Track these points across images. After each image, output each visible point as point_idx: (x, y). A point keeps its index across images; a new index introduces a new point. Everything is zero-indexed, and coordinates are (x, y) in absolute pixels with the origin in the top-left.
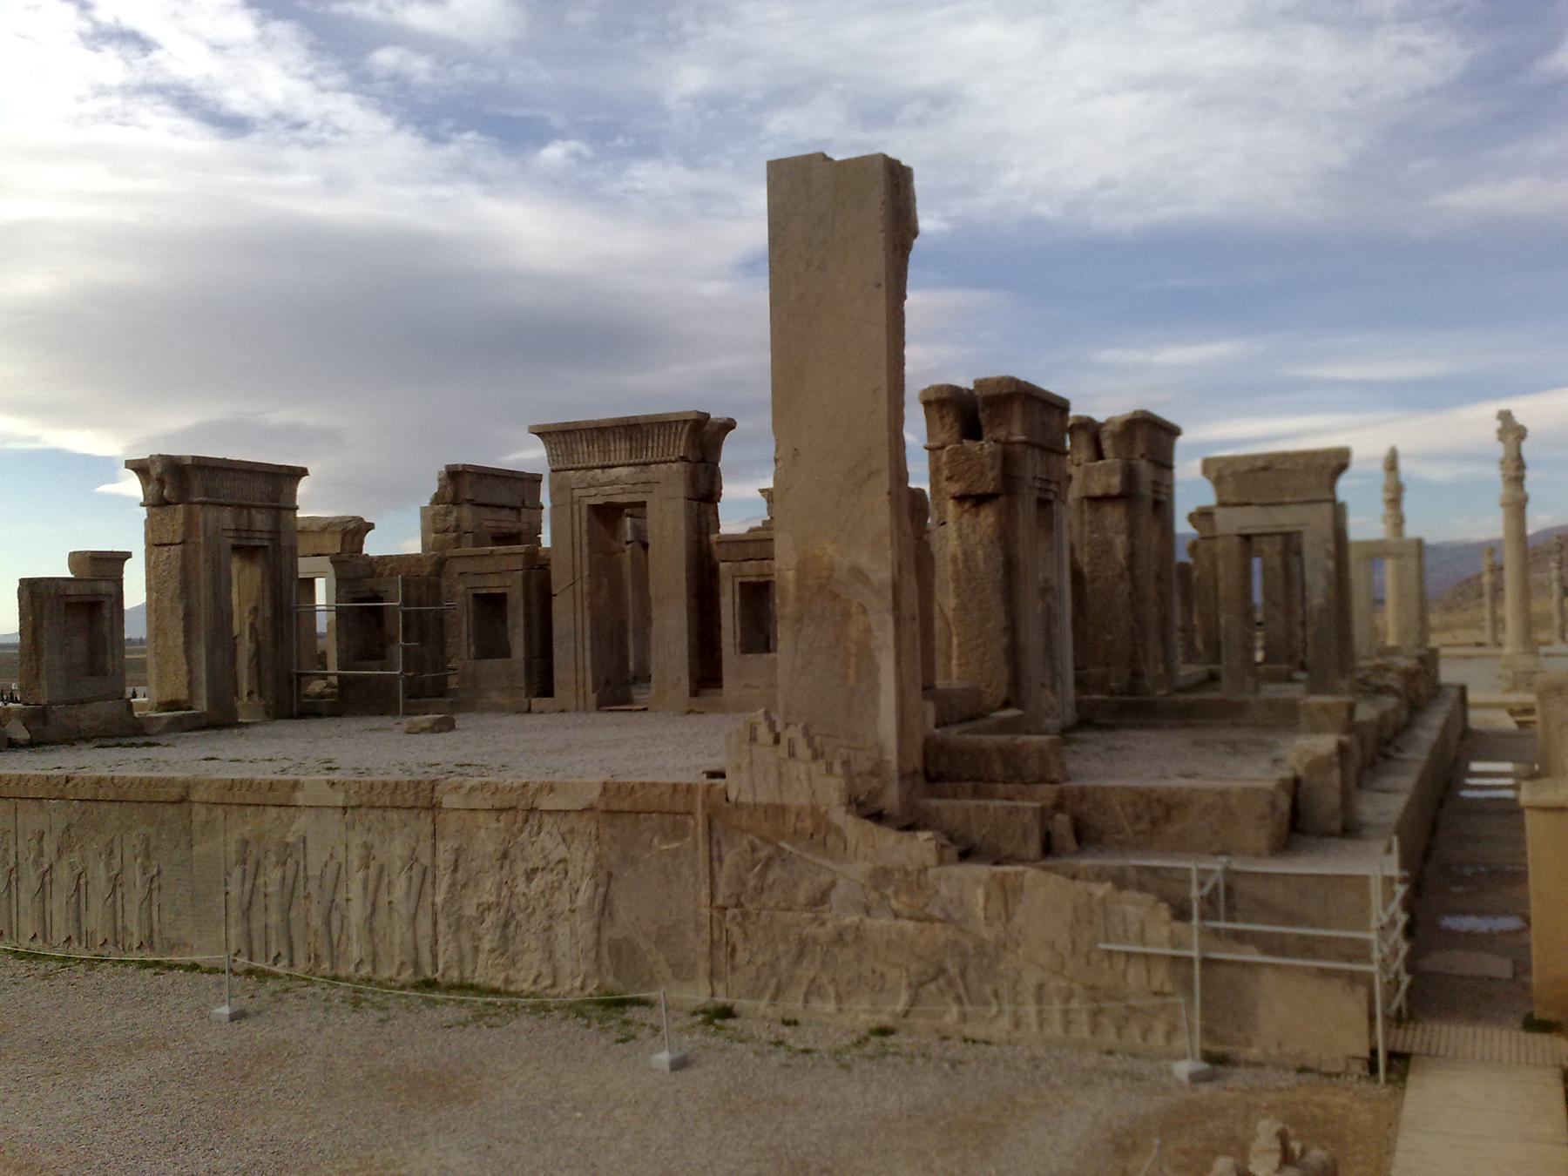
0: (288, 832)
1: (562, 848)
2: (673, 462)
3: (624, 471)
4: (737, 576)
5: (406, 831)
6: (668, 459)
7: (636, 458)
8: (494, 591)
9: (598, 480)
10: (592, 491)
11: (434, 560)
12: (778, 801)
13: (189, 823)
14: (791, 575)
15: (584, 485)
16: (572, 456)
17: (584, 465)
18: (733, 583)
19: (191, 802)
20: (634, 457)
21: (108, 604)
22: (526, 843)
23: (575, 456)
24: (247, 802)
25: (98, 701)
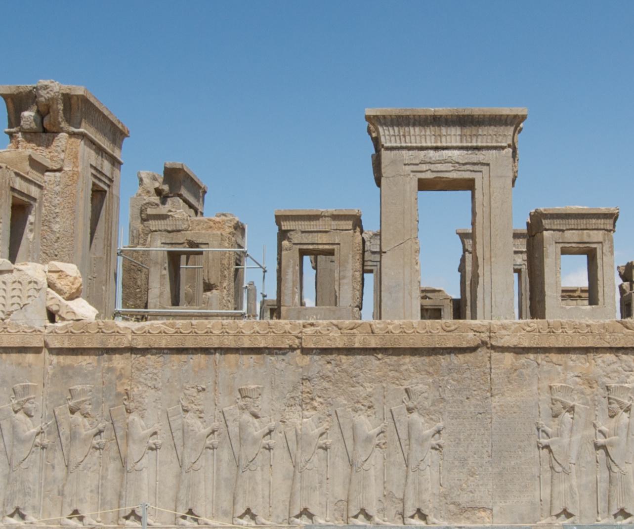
2: (503, 148)
3: (456, 153)
4: (559, 243)
6: (500, 144)
7: (466, 143)
8: (321, 247)
9: (430, 158)
10: (424, 167)
11: (233, 223)
13: (488, 371)
15: (417, 162)
16: (404, 136)
17: (419, 145)
18: (556, 247)
19: (493, 348)
20: (465, 141)
23: (408, 138)
24: (576, 345)
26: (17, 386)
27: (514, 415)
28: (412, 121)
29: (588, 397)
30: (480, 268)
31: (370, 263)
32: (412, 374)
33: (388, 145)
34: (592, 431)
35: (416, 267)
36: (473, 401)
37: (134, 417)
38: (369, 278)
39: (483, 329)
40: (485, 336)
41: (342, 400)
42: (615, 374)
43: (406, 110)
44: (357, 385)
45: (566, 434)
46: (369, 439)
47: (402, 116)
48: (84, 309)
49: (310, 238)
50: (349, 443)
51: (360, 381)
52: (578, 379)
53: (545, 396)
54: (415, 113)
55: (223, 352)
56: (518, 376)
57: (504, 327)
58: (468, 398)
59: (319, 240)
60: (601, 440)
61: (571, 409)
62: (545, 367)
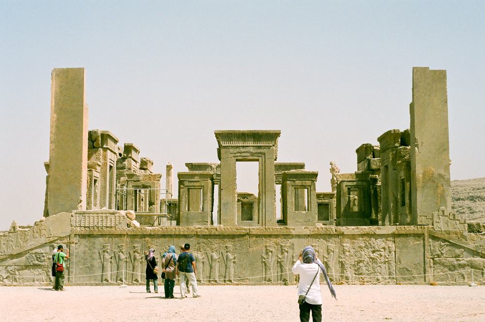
1: (384, 244)
5: (331, 241)
10: (239, 154)
12: (447, 230)
14: (421, 176)
21: (97, 181)
26: (119, 245)
30: (261, 196)
31: (216, 180)
33: (224, 145)
38: (216, 187)
40: (248, 231)
41: (208, 249)
45: (270, 258)
46: (216, 260)
48: (137, 224)
50: (210, 261)
53: (264, 248)
57: (253, 229)
60: (279, 260)
61: (272, 252)
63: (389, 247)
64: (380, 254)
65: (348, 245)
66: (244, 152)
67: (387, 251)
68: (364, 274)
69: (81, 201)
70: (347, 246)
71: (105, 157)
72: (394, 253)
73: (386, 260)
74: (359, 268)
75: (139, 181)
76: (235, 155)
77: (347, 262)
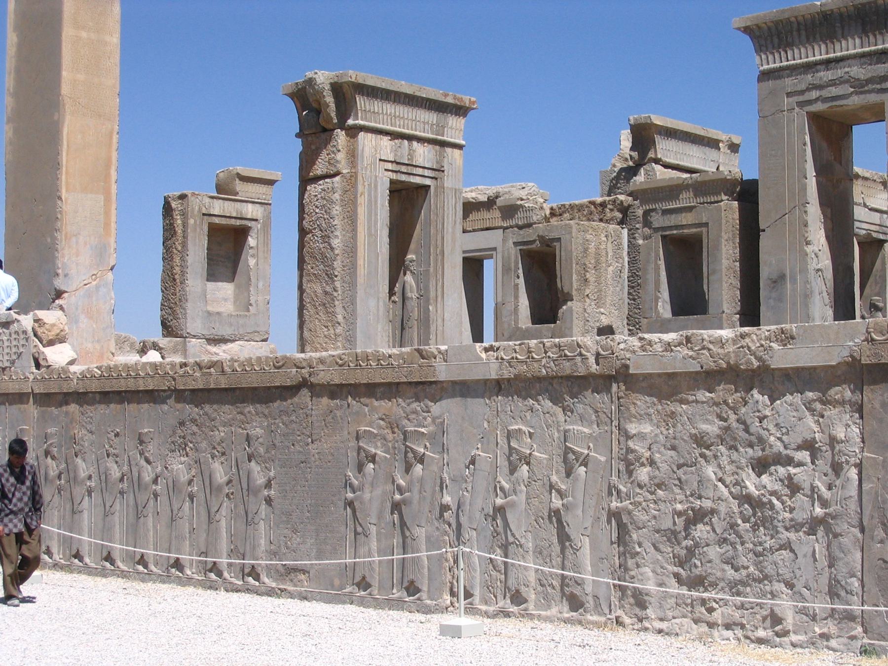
0: (425, 418)
5: (580, 407)
22: (749, 422)
25: (239, 340)
27: (329, 464)
28: (795, 26)
29: (390, 445)
32: (253, 417)
34: (389, 487)
35: (805, 248)
36: (298, 448)
37: (79, 461)
39: (304, 364)
42: (414, 416)
43: (783, 11)
44: (215, 429)
46: (219, 488)
47: (781, 21)
49: (673, 220)
50: (208, 491)
51: (216, 425)
52: (382, 423)
54: (796, 14)
55: (294, 390)
56: (333, 418)
58: (293, 445)
59: (683, 220)
62: (355, 408)
63: (833, 441)
64: (790, 477)
65: (647, 428)
66: (833, 83)
67: (823, 464)
68: (714, 585)
69: (59, 294)
70: (641, 436)
71: (353, 156)
72: (853, 473)
73: (819, 511)
74: (690, 551)
75: (529, 225)
76: (801, 98)
77: (640, 516)
